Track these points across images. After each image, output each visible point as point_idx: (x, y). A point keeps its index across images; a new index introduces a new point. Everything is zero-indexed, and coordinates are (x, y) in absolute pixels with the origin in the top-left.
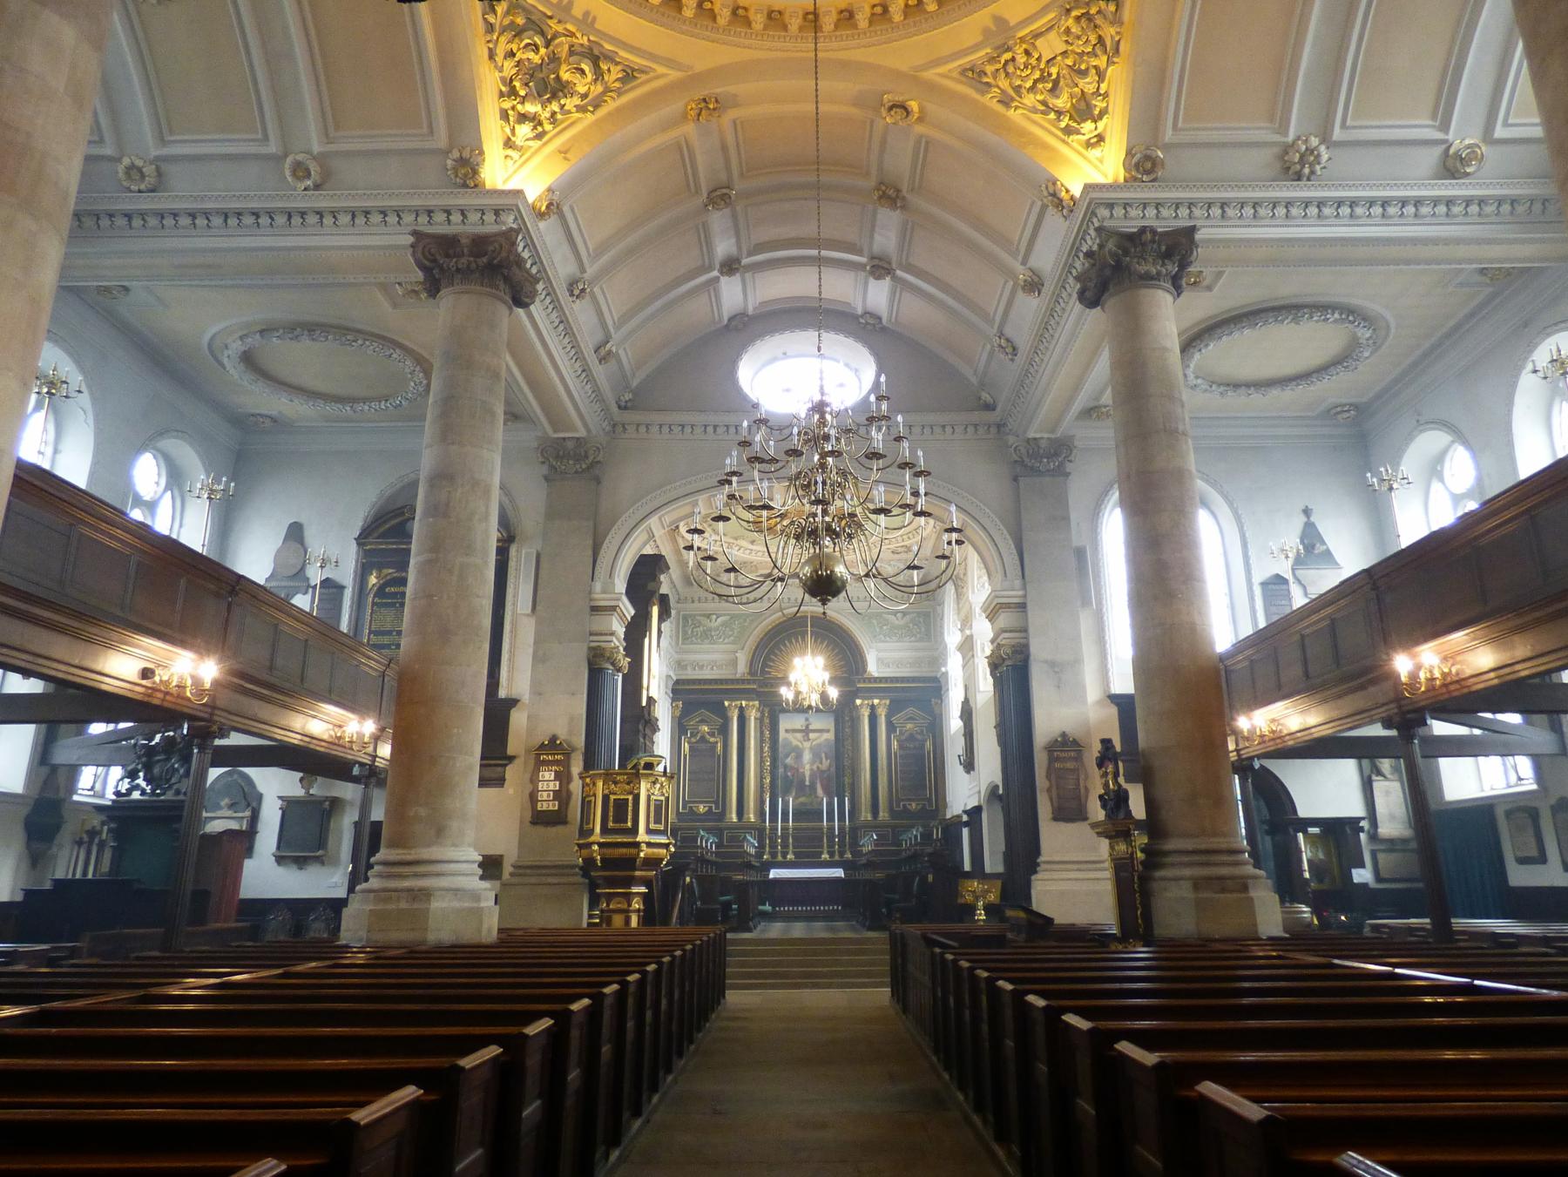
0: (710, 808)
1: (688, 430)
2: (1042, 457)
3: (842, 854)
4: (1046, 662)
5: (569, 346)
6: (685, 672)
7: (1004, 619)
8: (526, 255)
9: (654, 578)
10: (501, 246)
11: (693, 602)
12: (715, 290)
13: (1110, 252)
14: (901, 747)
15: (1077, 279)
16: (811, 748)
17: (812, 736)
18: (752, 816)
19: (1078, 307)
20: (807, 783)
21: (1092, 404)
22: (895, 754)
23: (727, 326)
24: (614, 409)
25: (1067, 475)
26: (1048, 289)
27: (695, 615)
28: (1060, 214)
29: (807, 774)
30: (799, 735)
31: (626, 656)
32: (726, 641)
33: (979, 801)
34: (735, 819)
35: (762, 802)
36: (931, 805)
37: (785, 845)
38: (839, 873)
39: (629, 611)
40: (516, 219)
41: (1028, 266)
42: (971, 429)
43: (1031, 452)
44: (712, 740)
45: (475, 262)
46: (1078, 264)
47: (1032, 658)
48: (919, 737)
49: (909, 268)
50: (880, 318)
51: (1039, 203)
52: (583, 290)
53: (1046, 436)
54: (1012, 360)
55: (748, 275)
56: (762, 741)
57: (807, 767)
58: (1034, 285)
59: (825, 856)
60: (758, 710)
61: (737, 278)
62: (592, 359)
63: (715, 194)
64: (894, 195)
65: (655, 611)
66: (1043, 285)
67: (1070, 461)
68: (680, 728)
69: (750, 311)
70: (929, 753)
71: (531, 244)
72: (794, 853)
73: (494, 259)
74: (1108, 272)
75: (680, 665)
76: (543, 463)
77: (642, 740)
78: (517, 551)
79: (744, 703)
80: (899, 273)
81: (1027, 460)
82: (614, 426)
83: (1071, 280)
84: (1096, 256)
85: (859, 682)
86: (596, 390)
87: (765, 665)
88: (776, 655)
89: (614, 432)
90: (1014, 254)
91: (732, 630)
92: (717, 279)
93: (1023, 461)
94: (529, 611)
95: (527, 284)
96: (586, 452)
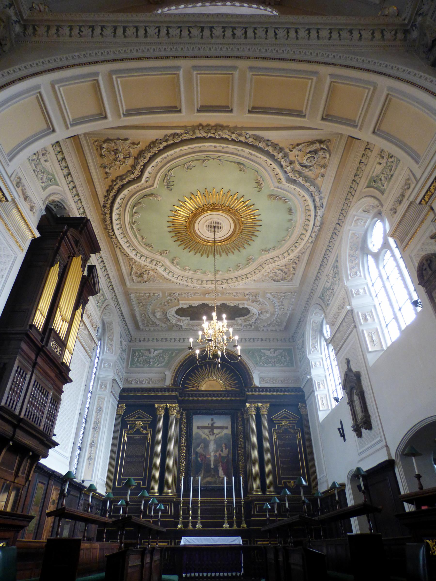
0: (139, 484)
3: (239, 525)
11: (140, 341)
14: (279, 438)
16: (215, 441)
17: (215, 431)
18: (170, 491)
20: (212, 466)
22: (276, 443)
27: (140, 350)
29: (212, 459)
30: (207, 431)
32: (159, 365)
35: (179, 481)
37: (195, 517)
38: (237, 540)
44: (144, 432)
48: (292, 431)
56: (180, 435)
57: (212, 454)
59: (226, 526)
60: (178, 412)
70: (299, 442)
72: (202, 523)
75: (127, 380)
85: (248, 391)
87: (184, 383)
88: (192, 377)
91: (164, 358)
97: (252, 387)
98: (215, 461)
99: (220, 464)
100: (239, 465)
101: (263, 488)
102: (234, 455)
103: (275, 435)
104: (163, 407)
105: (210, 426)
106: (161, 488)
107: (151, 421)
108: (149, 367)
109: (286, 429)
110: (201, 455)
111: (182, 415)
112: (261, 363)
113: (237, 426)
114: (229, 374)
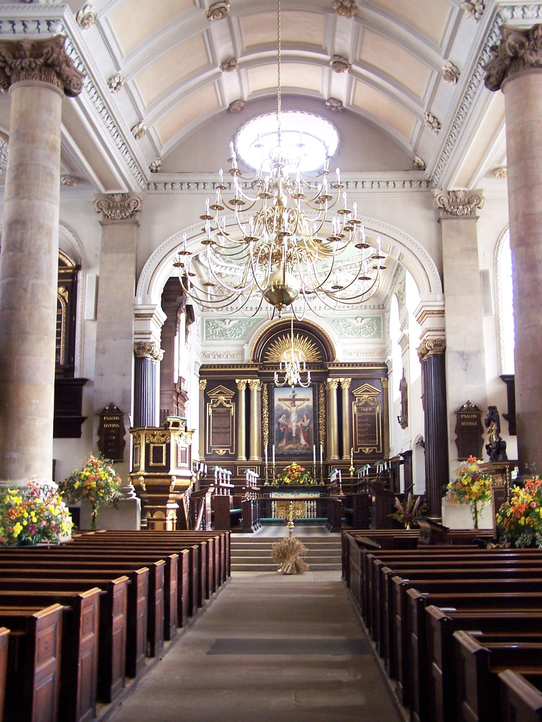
0: (228, 451)
1: (201, 186)
2: (459, 205)
4: (458, 352)
5: (112, 126)
6: (209, 359)
7: (431, 322)
8: (73, 56)
9: (181, 293)
10: (53, 49)
12: (218, 81)
13: (509, 44)
14: (359, 411)
15: (484, 68)
16: (297, 411)
17: (297, 403)
19: (486, 90)
20: (294, 435)
21: (496, 166)
22: (355, 415)
23: (229, 109)
24: (148, 173)
25: (478, 218)
26: (463, 78)
28: (473, 16)
29: (294, 429)
30: (288, 403)
31: (162, 348)
33: (411, 447)
34: (244, 458)
36: (379, 450)
39: (163, 317)
40: (63, 28)
41: (449, 59)
42: (407, 184)
43: (451, 201)
44: (228, 406)
45: (35, 62)
46: (486, 57)
47: (447, 350)
48: (372, 404)
49: (357, 63)
50: (341, 102)
51: (457, 10)
52: (119, 84)
53: (462, 189)
54: (437, 132)
55: (243, 71)
56: (262, 407)
57: (294, 424)
58: (453, 75)
61: (233, 74)
62: (130, 136)
63: (215, 7)
64: (349, 5)
65: (183, 317)
66: (460, 74)
67: (479, 208)
68: (206, 398)
69: (246, 99)
70: (378, 414)
71: (76, 48)
73: (48, 59)
74: (507, 62)
75: (204, 355)
76: (99, 212)
77: (175, 406)
78: (83, 275)
79: (249, 381)
80: (354, 67)
81: (447, 207)
82: (148, 184)
83: (480, 70)
84: (499, 48)
85: (330, 366)
86: (134, 159)
87: (264, 354)
89: (148, 189)
90: (438, 50)
92: (220, 73)
93: (445, 208)
94: (92, 317)
95: (74, 78)
96: (129, 205)
97: (334, 362)
98: (298, 430)
99: (301, 433)
100: (319, 434)
101: (340, 454)
102: (315, 426)
103: (355, 409)
104: (244, 382)
105: (291, 398)
106: (248, 455)
107: (234, 396)
108: (225, 339)
109: (366, 402)
110: (283, 425)
111: (262, 387)
112: (346, 334)
113: (319, 398)
114: (312, 344)
